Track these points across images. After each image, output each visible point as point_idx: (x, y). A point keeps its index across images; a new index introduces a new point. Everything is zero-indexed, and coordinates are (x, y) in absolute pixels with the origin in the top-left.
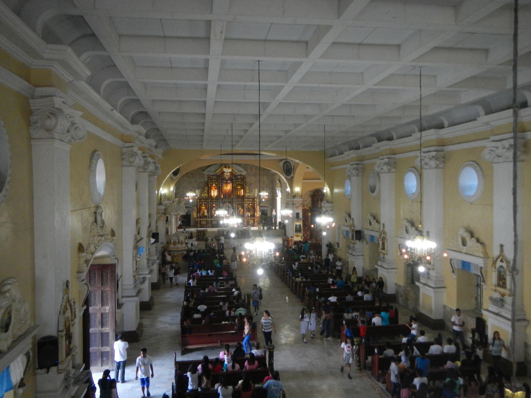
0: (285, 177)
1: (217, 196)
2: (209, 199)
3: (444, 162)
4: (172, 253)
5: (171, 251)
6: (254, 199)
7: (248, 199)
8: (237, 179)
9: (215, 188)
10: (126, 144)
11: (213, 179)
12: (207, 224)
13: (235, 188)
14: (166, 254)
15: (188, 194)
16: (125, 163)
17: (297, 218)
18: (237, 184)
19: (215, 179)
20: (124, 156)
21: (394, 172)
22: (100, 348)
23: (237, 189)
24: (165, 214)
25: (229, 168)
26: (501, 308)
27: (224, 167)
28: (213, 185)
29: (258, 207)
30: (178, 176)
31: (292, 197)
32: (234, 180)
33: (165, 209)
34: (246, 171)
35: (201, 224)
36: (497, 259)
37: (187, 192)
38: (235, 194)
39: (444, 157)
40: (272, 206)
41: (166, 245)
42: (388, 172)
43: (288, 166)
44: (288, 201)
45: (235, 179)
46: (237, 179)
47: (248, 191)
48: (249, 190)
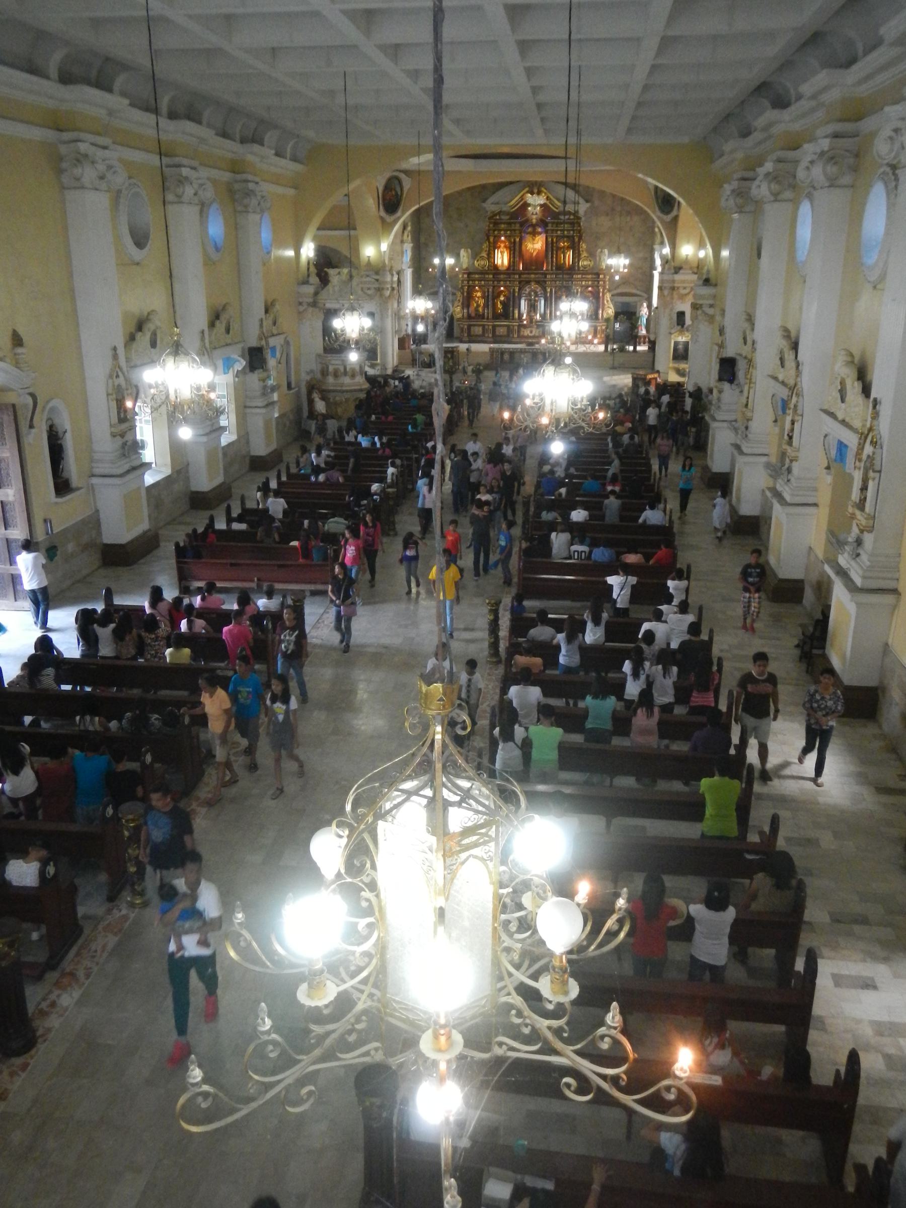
0: (659, 218)
1: (509, 268)
2: (488, 274)
3: (855, 169)
4: (331, 396)
5: (330, 391)
6: (598, 275)
7: (583, 274)
9: (505, 247)
10: (64, 134)
11: (501, 223)
12: (483, 335)
14: (316, 396)
16: (65, 179)
17: (678, 324)
18: (557, 237)
19: (504, 223)
20: (64, 165)
21: (791, 200)
22: (8, 566)
23: (558, 249)
24: (314, 304)
25: (539, 193)
26: (854, 559)
27: (528, 192)
28: (500, 237)
29: (608, 296)
30: (399, 214)
31: (673, 271)
32: (550, 225)
33: (316, 294)
34: (587, 201)
35: (472, 333)
36: (866, 438)
38: (552, 261)
39: (857, 156)
41: (319, 376)
42: (776, 200)
45: (553, 223)
46: (558, 224)
47: (584, 254)
48: (587, 251)
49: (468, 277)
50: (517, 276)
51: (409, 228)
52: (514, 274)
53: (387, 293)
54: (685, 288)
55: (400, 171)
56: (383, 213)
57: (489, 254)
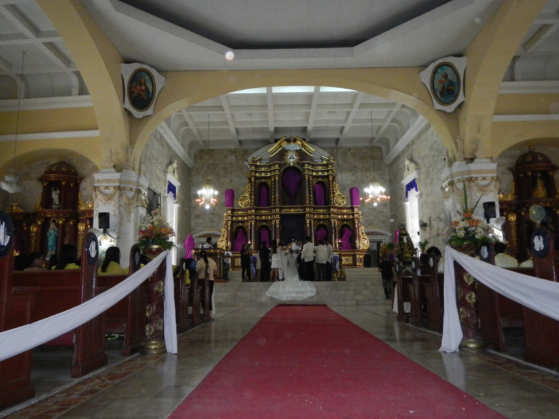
2: (250, 209)
8: (313, 165)
13: (309, 184)
15: (199, 192)
18: (314, 177)
25: (295, 141)
27: (284, 141)
30: (149, 111)
31: (464, 162)
32: (306, 166)
35: (236, 264)
37: (200, 188)
40: (392, 233)
43: (446, 76)
44: (452, 176)
46: (313, 165)
48: (341, 191)
49: (232, 213)
50: (278, 210)
51: (175, 165)
52: (275, 208)
53: (131, 194)
54: (484, 178)
55: (152, 67)
56: (128, 105)
57: (250, 195)
